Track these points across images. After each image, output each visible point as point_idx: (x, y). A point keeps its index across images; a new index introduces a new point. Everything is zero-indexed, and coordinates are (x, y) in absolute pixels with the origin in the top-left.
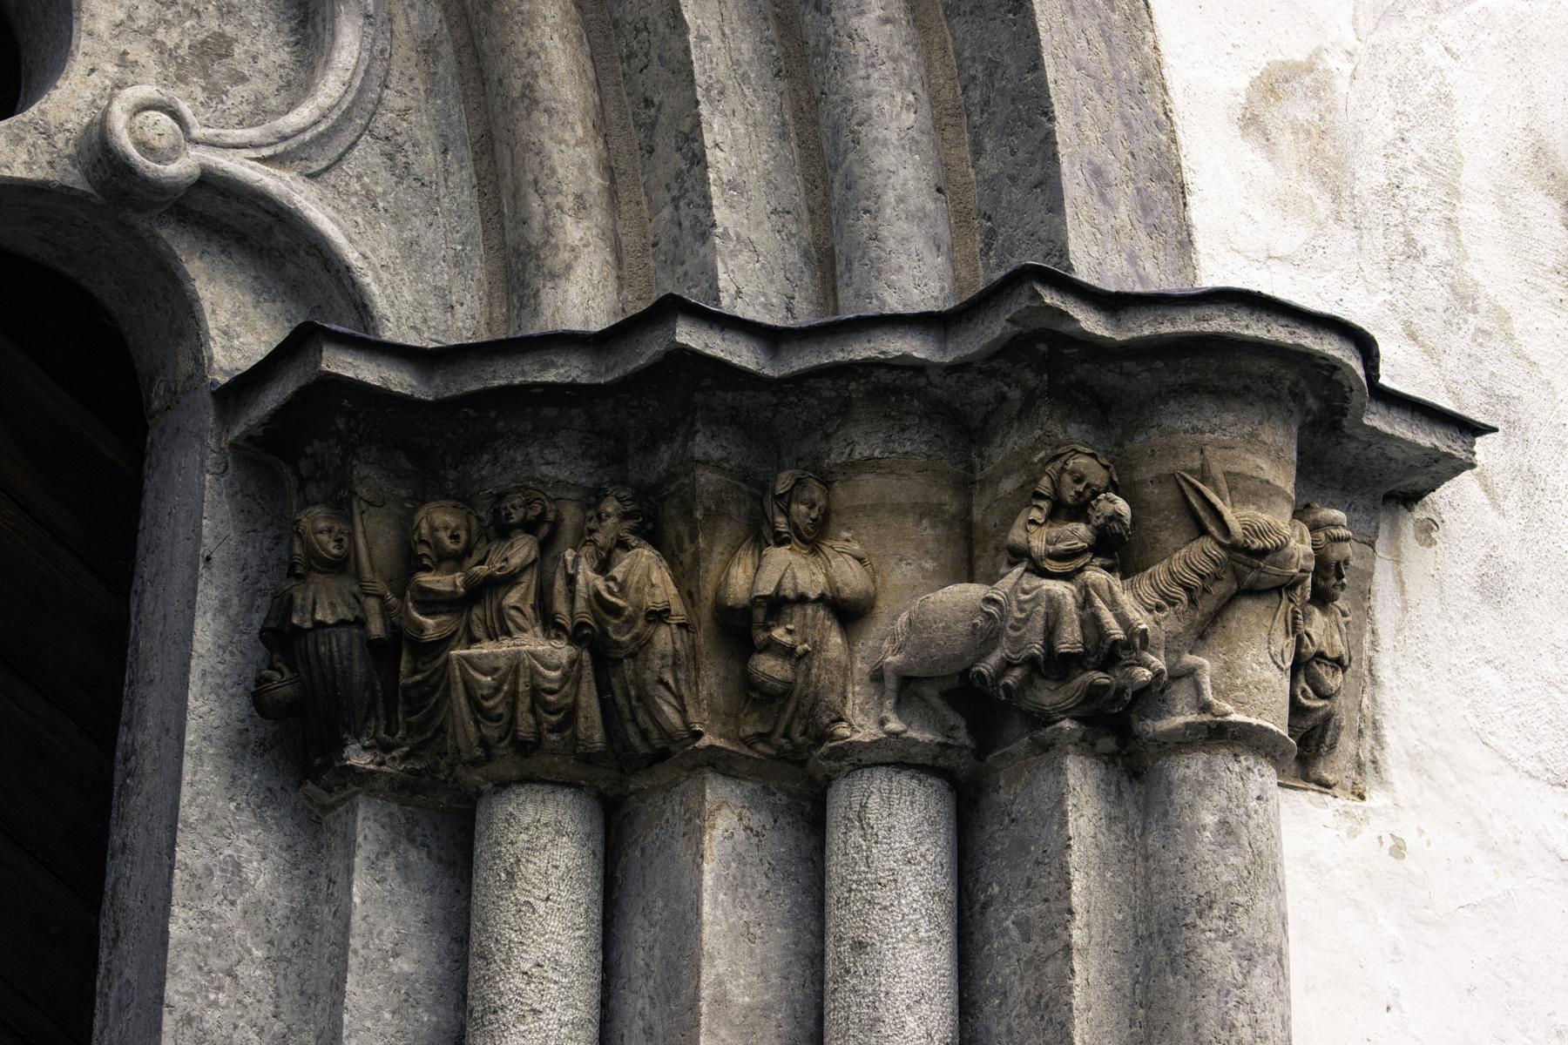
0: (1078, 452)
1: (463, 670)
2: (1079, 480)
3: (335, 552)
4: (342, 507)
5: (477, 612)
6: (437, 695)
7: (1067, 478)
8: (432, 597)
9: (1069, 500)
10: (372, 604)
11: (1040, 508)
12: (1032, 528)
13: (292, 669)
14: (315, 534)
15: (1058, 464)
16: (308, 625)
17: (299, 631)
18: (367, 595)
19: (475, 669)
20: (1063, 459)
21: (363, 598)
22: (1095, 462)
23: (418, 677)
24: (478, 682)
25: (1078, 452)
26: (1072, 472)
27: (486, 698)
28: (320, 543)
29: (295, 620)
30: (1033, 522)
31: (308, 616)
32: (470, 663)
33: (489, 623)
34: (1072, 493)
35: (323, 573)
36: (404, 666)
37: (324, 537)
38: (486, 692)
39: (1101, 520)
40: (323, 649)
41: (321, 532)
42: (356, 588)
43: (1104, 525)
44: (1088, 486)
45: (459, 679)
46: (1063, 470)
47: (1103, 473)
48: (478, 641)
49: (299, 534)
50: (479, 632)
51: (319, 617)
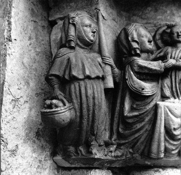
1: (166, 114)
3: (92, 38)
4: (95, 16)
5: (167, 82)
6: (143, 123)
8: (146, 71)
10: (108, 68)
13: (70, 101)
14: (83, 26)
16: (81, 77)
17: (75, 79)
18: (106, 64)
19: (172, 113)
21: (103, 65)
23: (136, 113)
24: (172, 120)
27: (175, 129)
28: (85, 32)
29: (74, 73)
31: (81, 72)
32: (170, 111)
33: (174, 89)
35: (83, 48)
36: (127, 106)
37: (88, 29)
38: (176, 127)
40: (90, 92)
41: (86, 26)
42: (100, 59)
45: (163, 118)
48: (168, 98)
49: (74, 25)
50: (168, 93)
51: (88, 73)
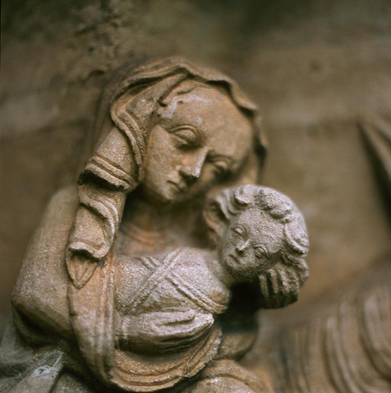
0: (191, 77)
2: (190, 147)
7: (163, 140)
9: (167, 192)
11: (101, 218)
12: (78, 269)
15: (145, 106)
20: (157, 90)
22: (226, 101)
25: (191, 77)
26: (174, 128)
30: (83, 255)
34: (174, 176)
39: (249, 260)
43: (261, 270)
44: (209, 159)
46: (155, 119)
47: (244, 128)
